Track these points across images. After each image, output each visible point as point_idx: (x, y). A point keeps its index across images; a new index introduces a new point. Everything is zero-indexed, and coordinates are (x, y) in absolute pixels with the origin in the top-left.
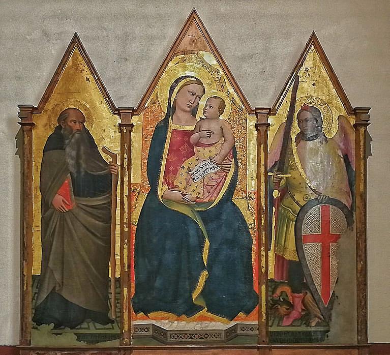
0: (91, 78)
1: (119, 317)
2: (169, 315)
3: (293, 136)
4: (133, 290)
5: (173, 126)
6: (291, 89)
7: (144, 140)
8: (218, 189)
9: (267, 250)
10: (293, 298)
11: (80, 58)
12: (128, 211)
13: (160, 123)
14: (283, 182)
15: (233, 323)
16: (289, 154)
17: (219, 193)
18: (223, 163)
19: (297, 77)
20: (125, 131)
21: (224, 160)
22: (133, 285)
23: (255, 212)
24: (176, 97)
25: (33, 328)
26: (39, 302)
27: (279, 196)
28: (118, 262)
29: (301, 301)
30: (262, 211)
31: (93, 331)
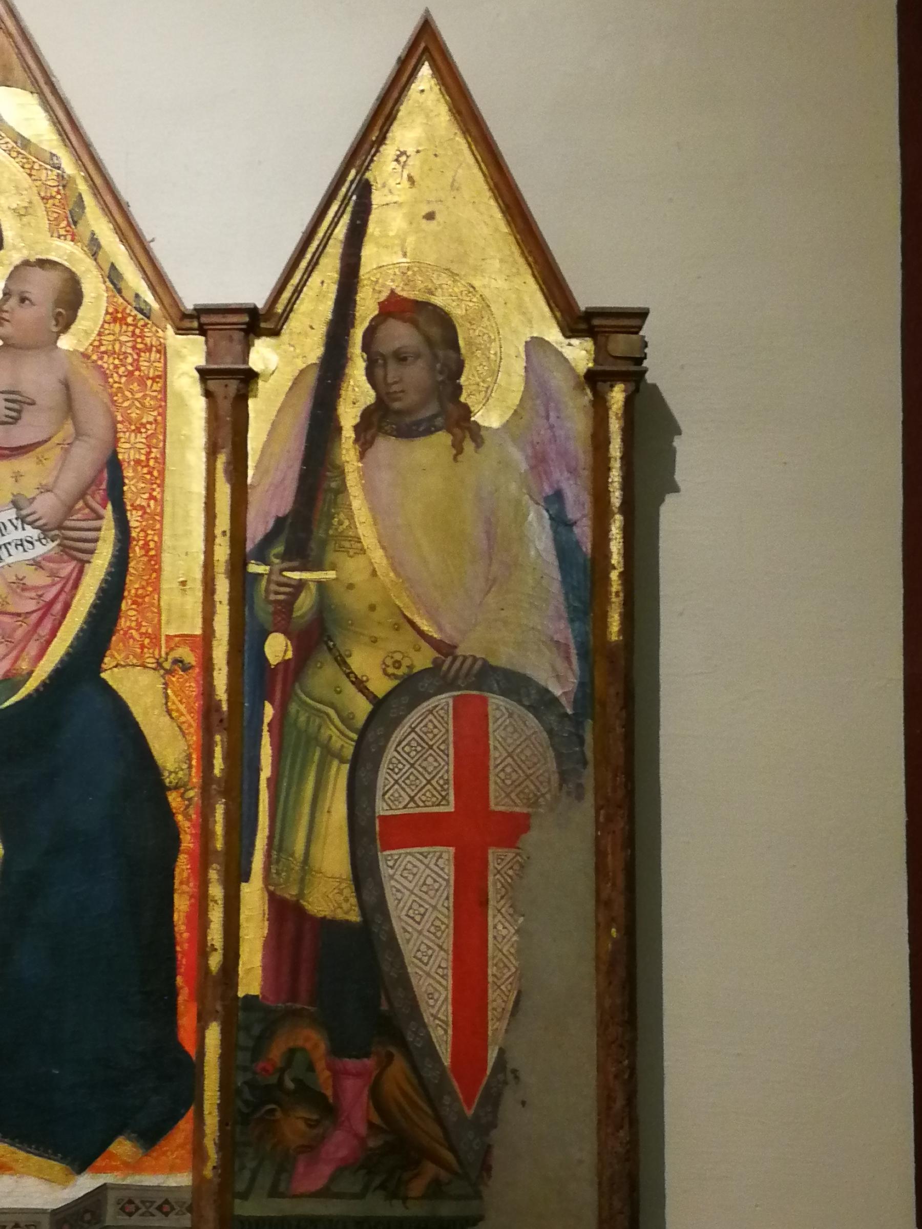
3: (349, 415)
6: (341, 231)
8: (44, 630)
9: (236, 874)
10: (337, 1075)
14: (305, 603)
15: (86, 1183)
16: (330, 490)
17: (49, 642)
18: (68, 523)
19: (365, 190)
21: (70, 510)
23: (190, 720)
27: (290, 655)
29: (366, 1092)
30: (215, 718)
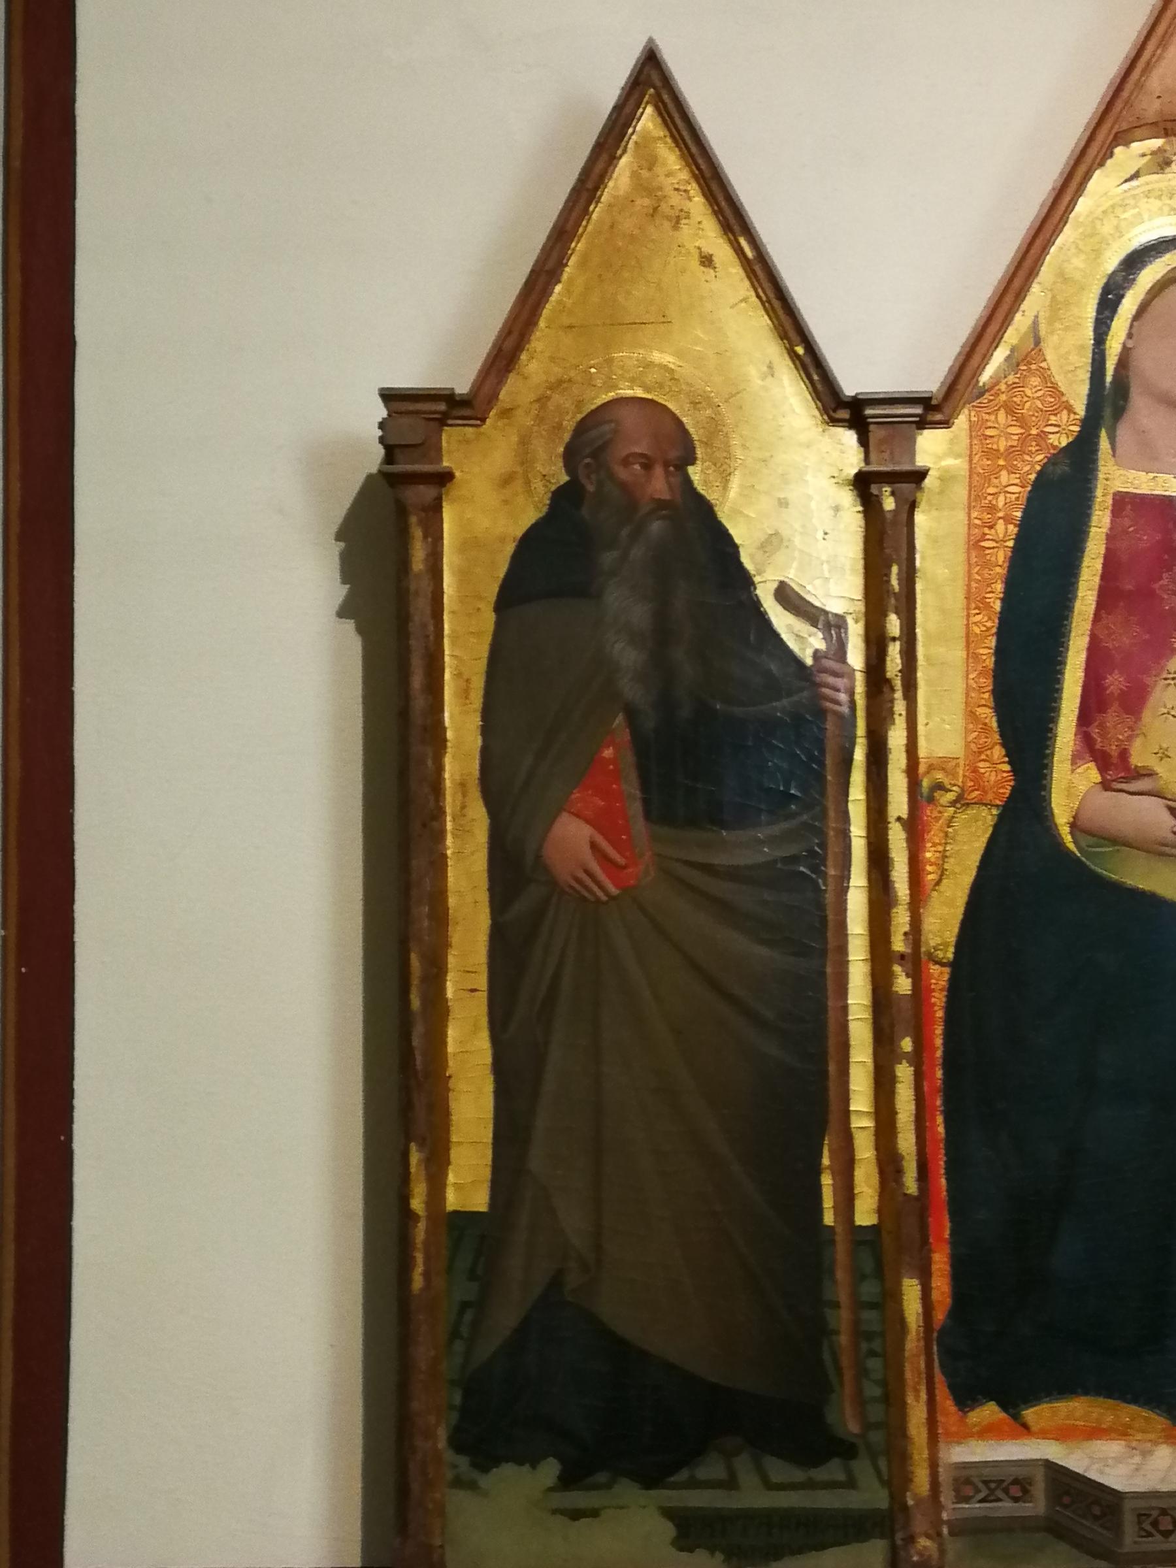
0: (722, 251)
1: (877, 1426)
2: (1128, 1412)
4: (941, 1286)
5: (1117, 476)
7: (975, 545)
11: (670, 159)
12: (901, 893)
13: (1052, 461)
20: (889, 504)
22: (940, 1261)
24: (1130, 336)
25: (458, 1483)
26: (485, 1351)
28: (865, 1150)
31: (752, 1496)
